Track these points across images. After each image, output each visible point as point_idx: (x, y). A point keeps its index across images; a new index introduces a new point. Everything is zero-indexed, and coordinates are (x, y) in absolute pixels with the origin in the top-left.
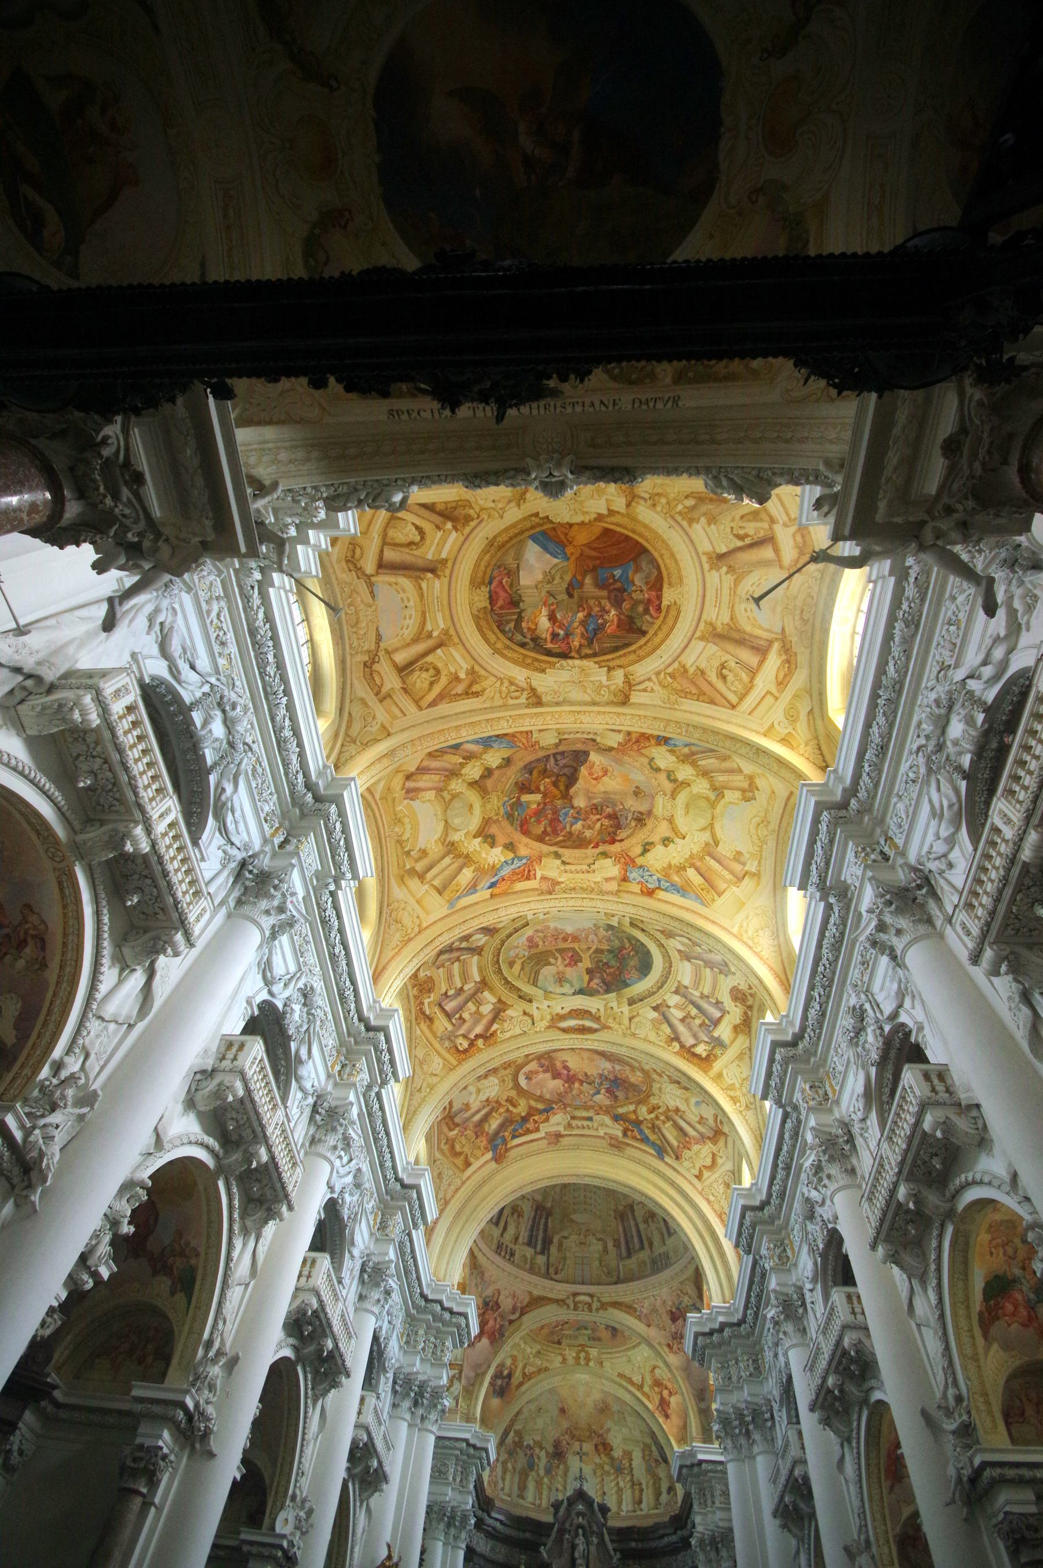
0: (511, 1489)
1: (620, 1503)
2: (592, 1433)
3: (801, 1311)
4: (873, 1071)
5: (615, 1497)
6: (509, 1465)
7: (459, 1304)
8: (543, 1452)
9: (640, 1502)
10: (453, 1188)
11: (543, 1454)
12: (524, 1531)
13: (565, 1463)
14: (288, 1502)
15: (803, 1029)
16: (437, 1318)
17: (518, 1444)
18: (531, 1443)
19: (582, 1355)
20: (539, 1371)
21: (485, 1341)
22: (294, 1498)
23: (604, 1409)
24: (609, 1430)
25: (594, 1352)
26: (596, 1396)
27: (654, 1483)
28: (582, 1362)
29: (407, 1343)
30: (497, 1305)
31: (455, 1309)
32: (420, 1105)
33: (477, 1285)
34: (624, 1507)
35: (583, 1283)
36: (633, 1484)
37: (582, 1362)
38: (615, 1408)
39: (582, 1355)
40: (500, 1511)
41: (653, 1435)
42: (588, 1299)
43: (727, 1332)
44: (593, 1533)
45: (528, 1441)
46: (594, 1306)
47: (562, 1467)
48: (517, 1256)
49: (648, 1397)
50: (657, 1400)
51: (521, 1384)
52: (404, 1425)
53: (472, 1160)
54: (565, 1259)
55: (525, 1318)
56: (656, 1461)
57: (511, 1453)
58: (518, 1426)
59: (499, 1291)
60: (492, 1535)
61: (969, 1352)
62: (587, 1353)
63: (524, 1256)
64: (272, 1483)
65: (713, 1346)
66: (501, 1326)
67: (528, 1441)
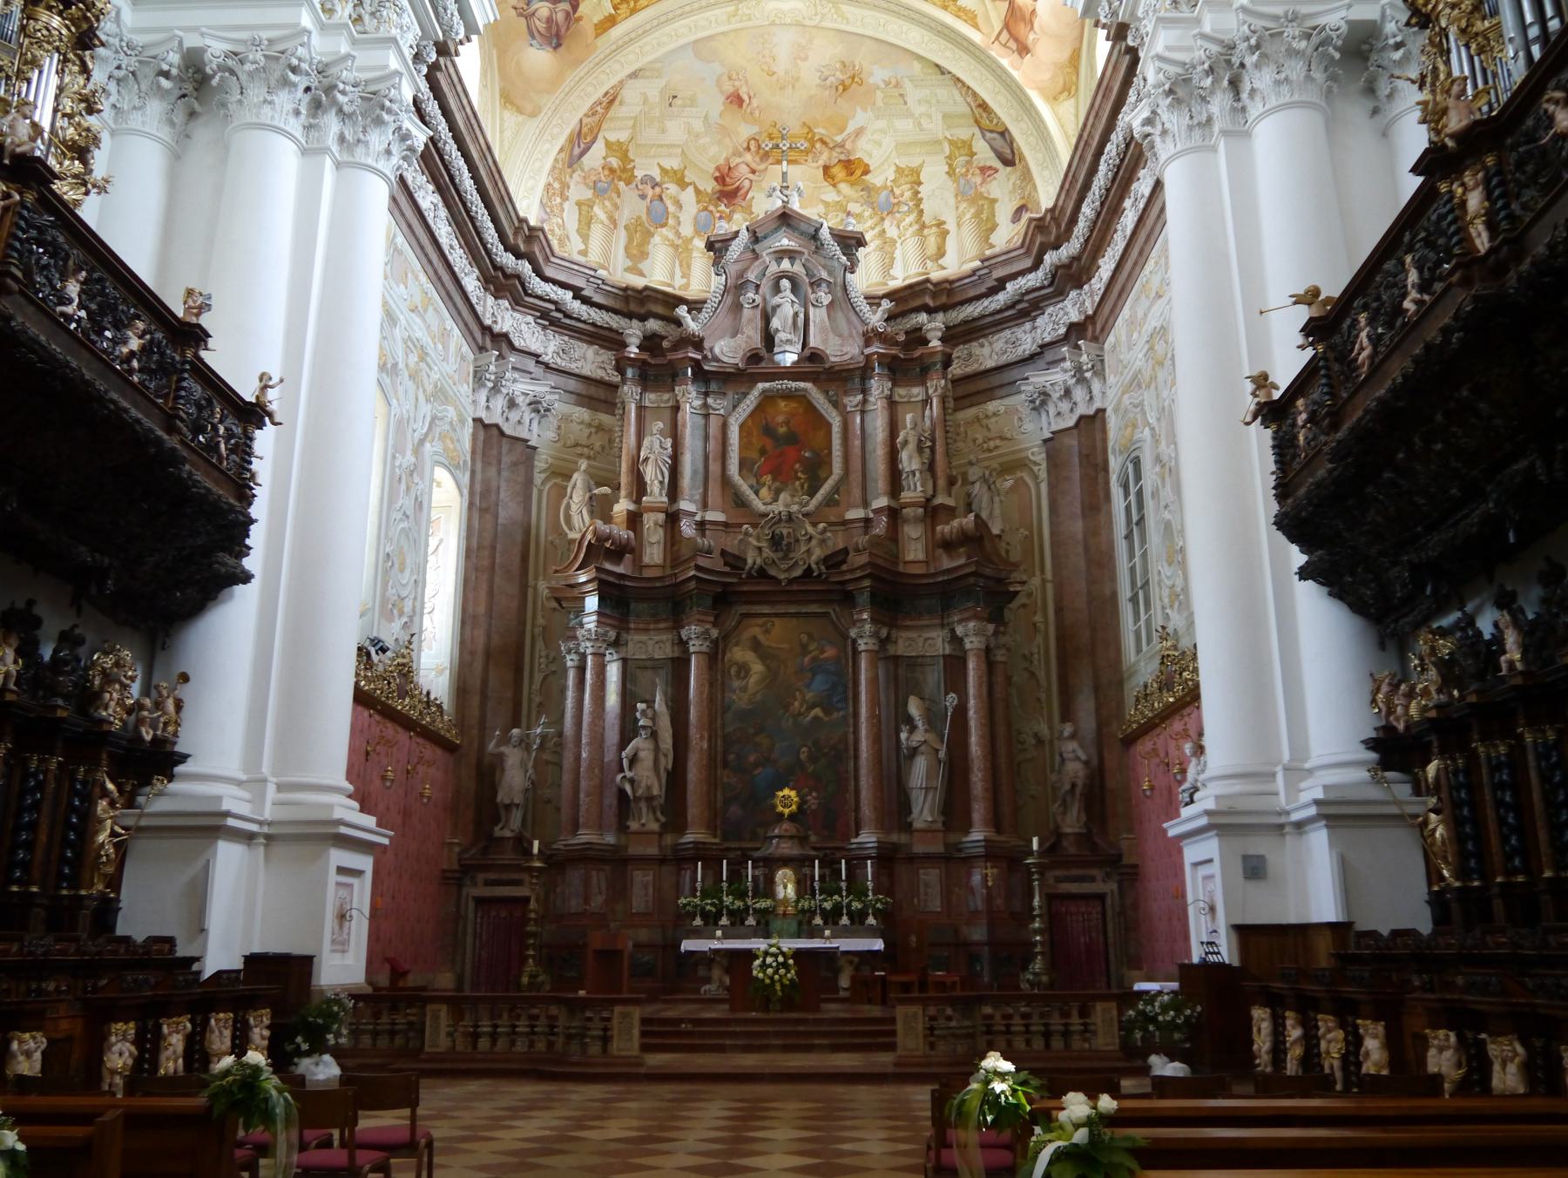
0: (606, 254)
6: (598, 211)
8: (690, 189)
9: (941, 253)
11: (688, 196)
17: (621, 172)
18: (656, 174)
23: (848, 84)
24: (859, 132)
26: (825, 53)
27: (977, 215)
36: (923, 226)
38: (878, 75)
45: (645, 167)
51: (611, 21)
56: (983, 170)
57: (599, 191)
58: (615, 132)
60: (552, 318)
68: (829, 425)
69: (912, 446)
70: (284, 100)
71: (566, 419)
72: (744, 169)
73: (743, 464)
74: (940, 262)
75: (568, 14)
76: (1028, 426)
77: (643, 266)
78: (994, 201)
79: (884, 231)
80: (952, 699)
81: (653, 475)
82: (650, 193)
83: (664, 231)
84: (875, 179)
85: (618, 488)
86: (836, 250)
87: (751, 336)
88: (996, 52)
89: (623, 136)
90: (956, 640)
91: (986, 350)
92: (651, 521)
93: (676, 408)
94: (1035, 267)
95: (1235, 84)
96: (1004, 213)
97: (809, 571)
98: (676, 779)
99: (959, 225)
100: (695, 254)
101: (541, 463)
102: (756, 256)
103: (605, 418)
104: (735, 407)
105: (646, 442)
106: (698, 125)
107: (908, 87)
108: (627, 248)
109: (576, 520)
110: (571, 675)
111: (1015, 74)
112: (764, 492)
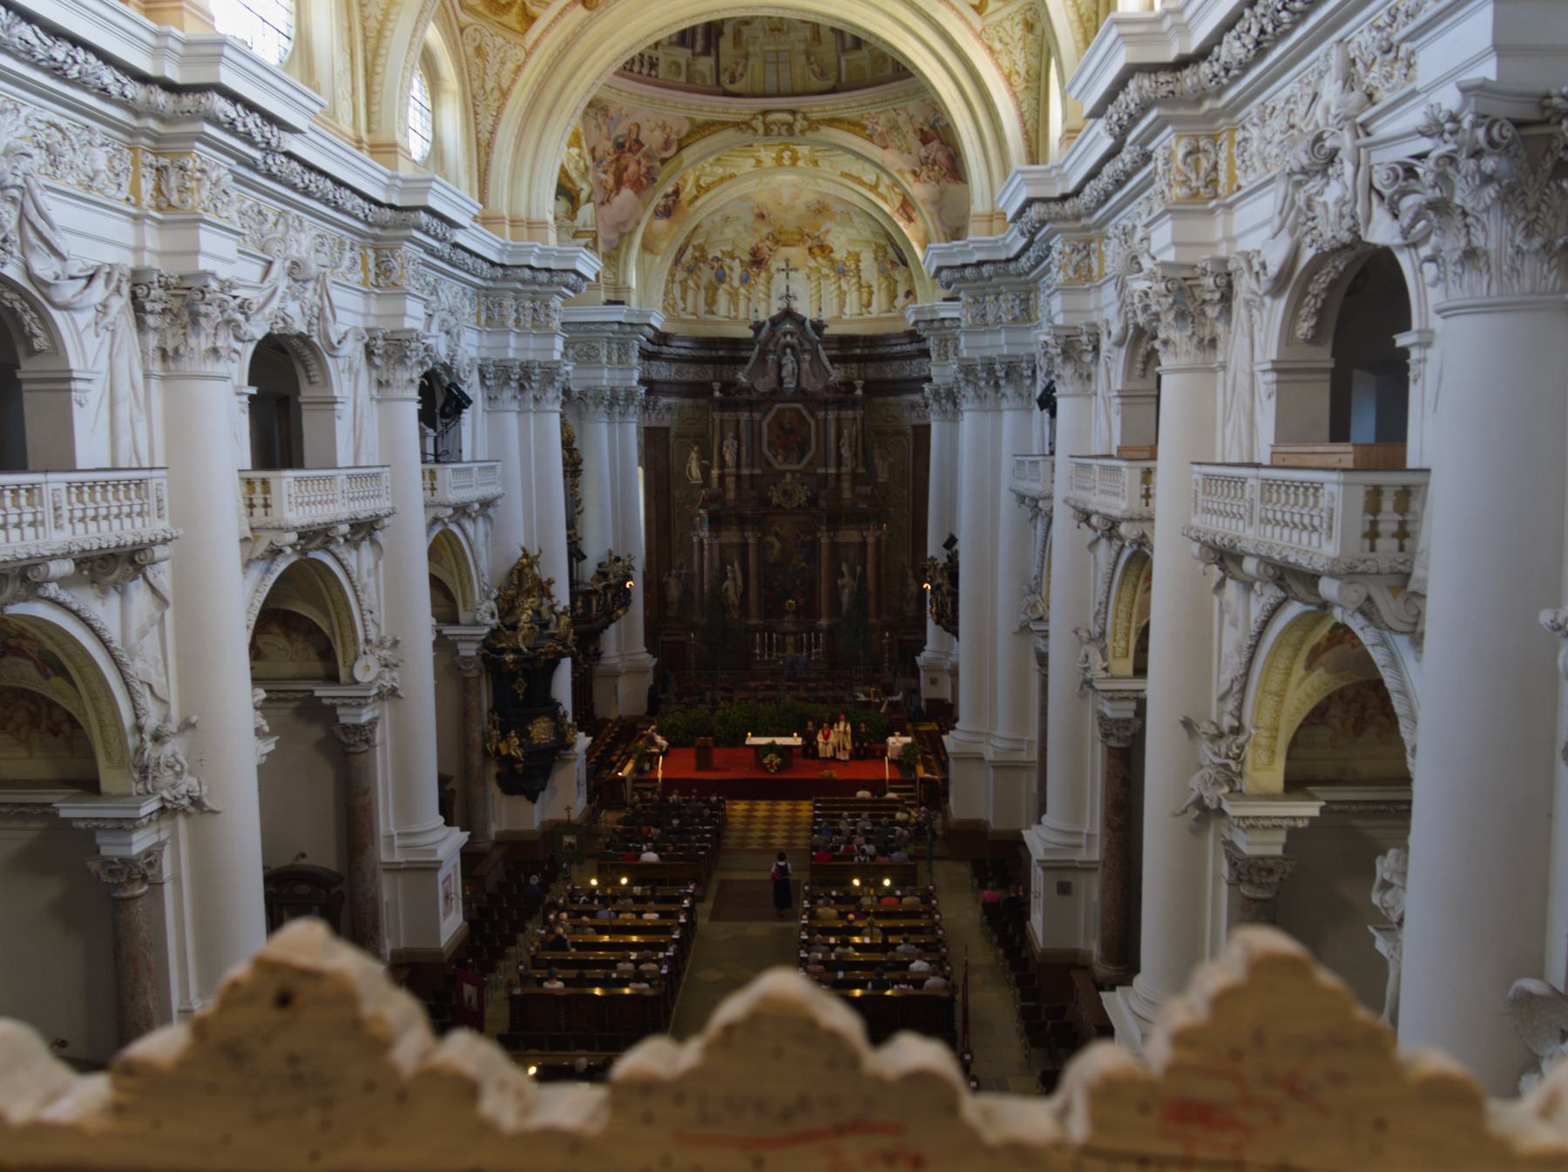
0: (695, 307)
1: (842, 305)
2: (802, 235)
3: (1088, 358)
4: (1308, 254)
5: (835, 301)
6: (691, 283)
7: (558, 259)
8: (737, 261)
9: (869, 304)
10: (510, 66)
11: (736, 264)
12: (717, 350)
13: (768, 270)
14: (362, 647)
15: (1203, 54)
16: (523, 282)
18: (719, 255)
19: (787, 154)
20: (722, 180)
21: (626, 192)
22: (368, 641)
23: (821, 210)
24: (827, 232)
25: (803, 150)
26: (809, 196)
28: (787, 162)
29: (489, 318)
30: (639, 143)
31: (553, 267)
32: (386, 14)
33: (599, 127)
34: (847, 310)
35: (779, 94)
36: (861, 286)
37: (787, 162)
38: (838, 208)
39: (787, 154)
40: (684, 339)
41: (889, 237)
42: (788, 117)
43: (986, 270)
44: (805, 351)
45: (714, 252)
46: (798, 127)
47: (763, 274)
48: (662, 69)
49: (885, 199)
50: (897, 202)
51: (696, 198)
52: (512, 421)
53: (534, 10)
54: (746, 57)
55: (686, 153)
56: (892, 263)
57: (690, 270)
59: (638, 126)
61: (1274, 686)
62: (794, 152)
63: (677, 65)
64: (333, 633)
65: (964, 279)
66: (649, 169)
67: (714, 252)
68: (809, 425)
69: (847, 446)
70: (602, 409)
71: (682, 407)
72: (766, 249)
73: (770, 444)
74: (870, 309)
75: (674, 202)
76: (906, 415)
77: (715, 309)
78: (896, 282)
79: (840, 286)
80: (859, 568)
81: (729, 458)
82: (716, 265)
83: (725, 286)
84: (837, 256)
85: (710, 459)
86: (812, 334)
87: (772, 375)
88: (897, 218)
89: (701, 241)
90: (864, 538)
91: (888, 369)
92: (730, 482)
93: (738, 421)
94: (911, 343)
95: (955, 404)
96: (901, 290)
97: (799, 506)
98: (744, 596)
99: (879, 290)
100: (741, 297)
101: (672, 434)
102: (774, 335)
103: (701, 401)
104: (765, 415)
105: (725, 443)
106: (741, 228)
107: (853, 214)
108: (706, 300)
109: (694, 473)
110: (696, 547)
111: (906, 232)
112: (780, 458)
